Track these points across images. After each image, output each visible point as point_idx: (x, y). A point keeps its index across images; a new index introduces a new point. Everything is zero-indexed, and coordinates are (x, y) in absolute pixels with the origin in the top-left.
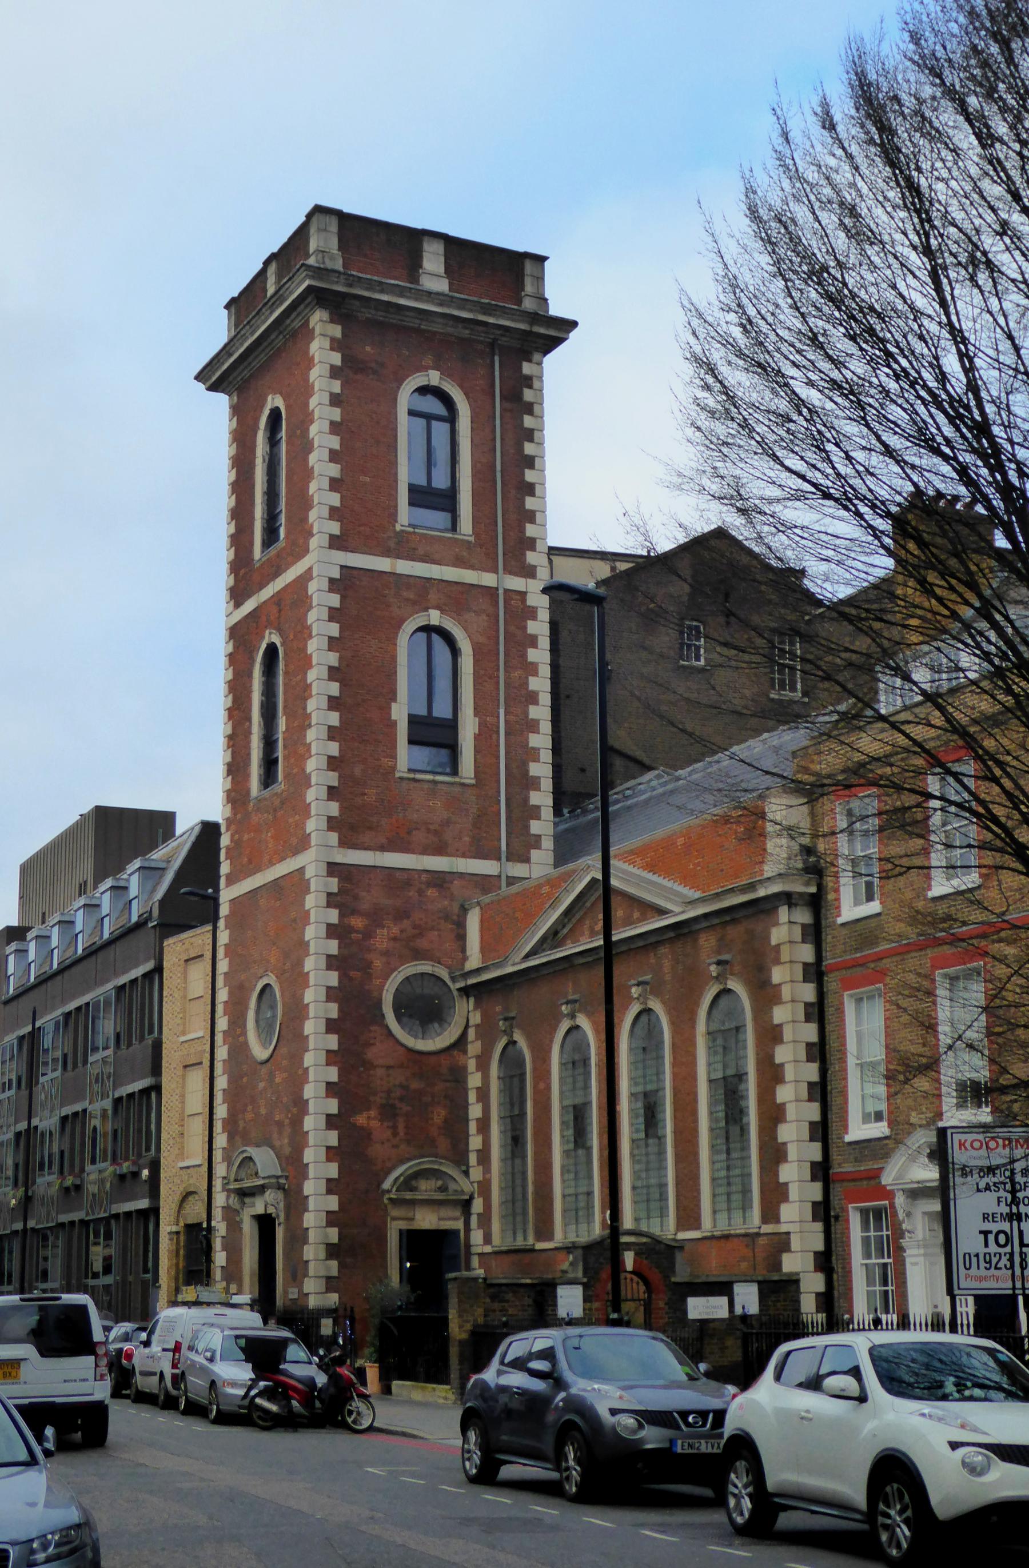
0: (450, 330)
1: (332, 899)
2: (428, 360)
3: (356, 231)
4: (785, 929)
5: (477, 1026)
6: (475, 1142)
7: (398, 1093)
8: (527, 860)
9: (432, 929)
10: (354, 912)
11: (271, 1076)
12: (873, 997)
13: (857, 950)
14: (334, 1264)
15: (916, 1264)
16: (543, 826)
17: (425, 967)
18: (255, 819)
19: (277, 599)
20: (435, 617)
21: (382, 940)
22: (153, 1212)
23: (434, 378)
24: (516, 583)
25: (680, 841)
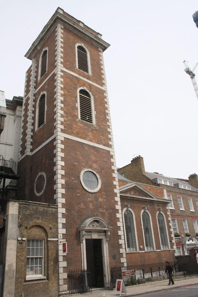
11: (96, 199)
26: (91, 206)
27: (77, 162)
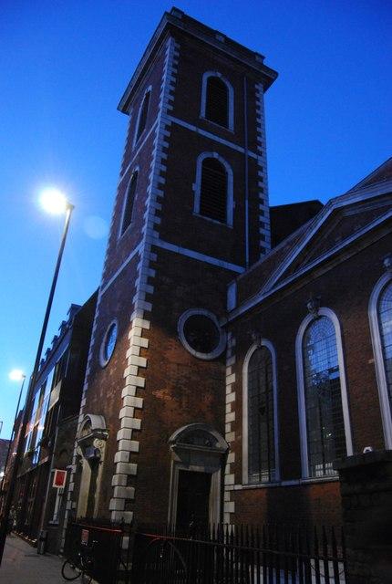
1: (151, 265)
6: (230, 417)
17: (205, 313)
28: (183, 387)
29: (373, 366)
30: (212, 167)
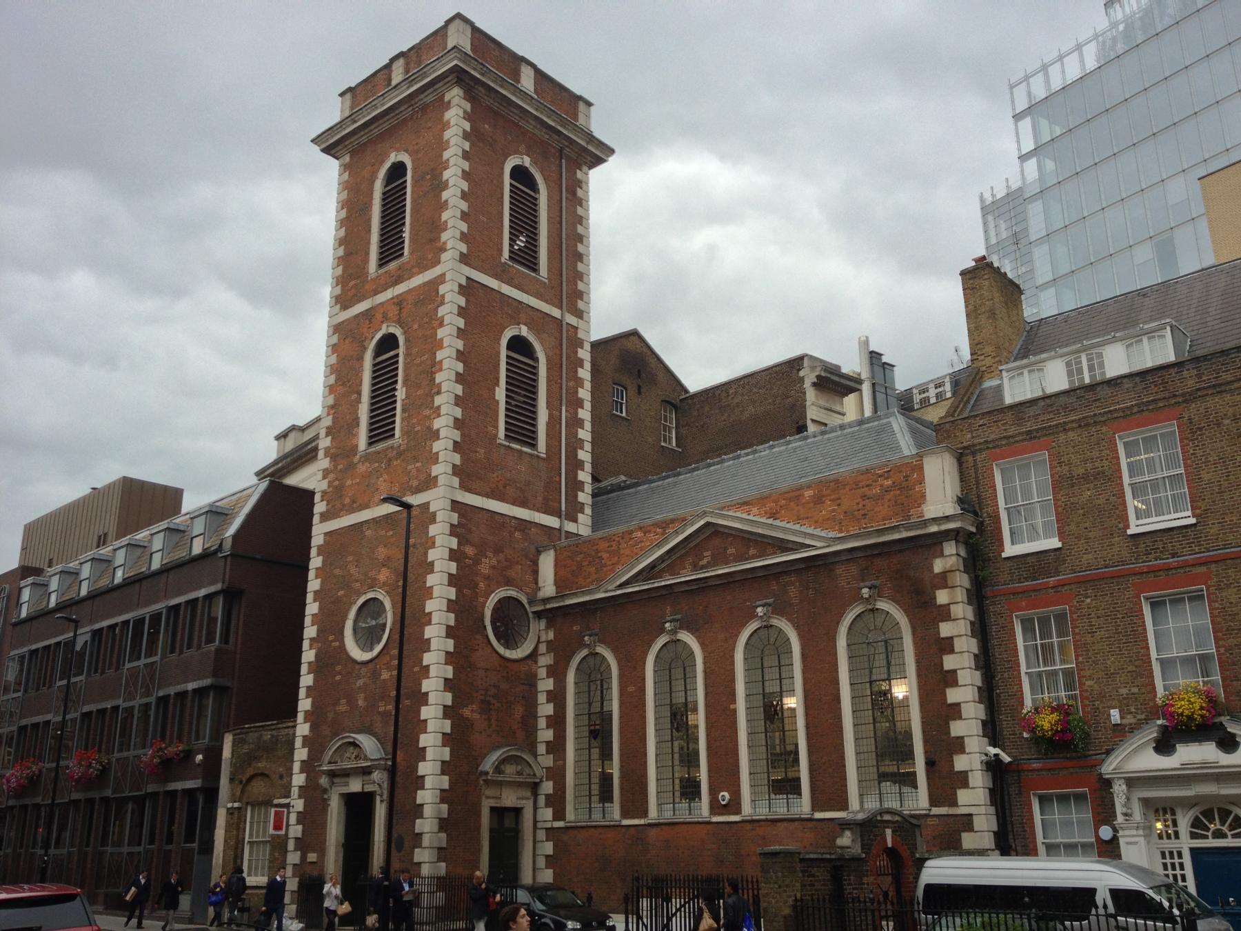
0: (536, 132)
2: (522, 148)
3: (481, 39)
4: (949, 558)
5: (549, 642)
7: (493, 691)
8: (575, 520)
9: (517, 563)
10: (468, 542)
11: (375, 675)
12: (1182, 600)
13: (1026, 579)
14: (443, 835)
15: (1136, 843)
16: (584, 497)
18: (362, 468)
19: (399, 301)
20: (524, 331)
21: (484, 568)
22: (211, 793)
23: (527, 161)
24: (571, 319)
25: (808, 493)
26: (361, 703)
27: (342, 589)
28: (493, 701)
29: (735, 711)
30: (519, 345)
